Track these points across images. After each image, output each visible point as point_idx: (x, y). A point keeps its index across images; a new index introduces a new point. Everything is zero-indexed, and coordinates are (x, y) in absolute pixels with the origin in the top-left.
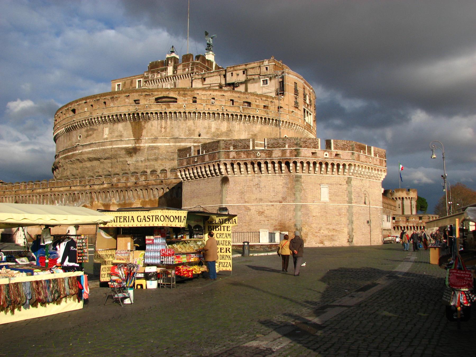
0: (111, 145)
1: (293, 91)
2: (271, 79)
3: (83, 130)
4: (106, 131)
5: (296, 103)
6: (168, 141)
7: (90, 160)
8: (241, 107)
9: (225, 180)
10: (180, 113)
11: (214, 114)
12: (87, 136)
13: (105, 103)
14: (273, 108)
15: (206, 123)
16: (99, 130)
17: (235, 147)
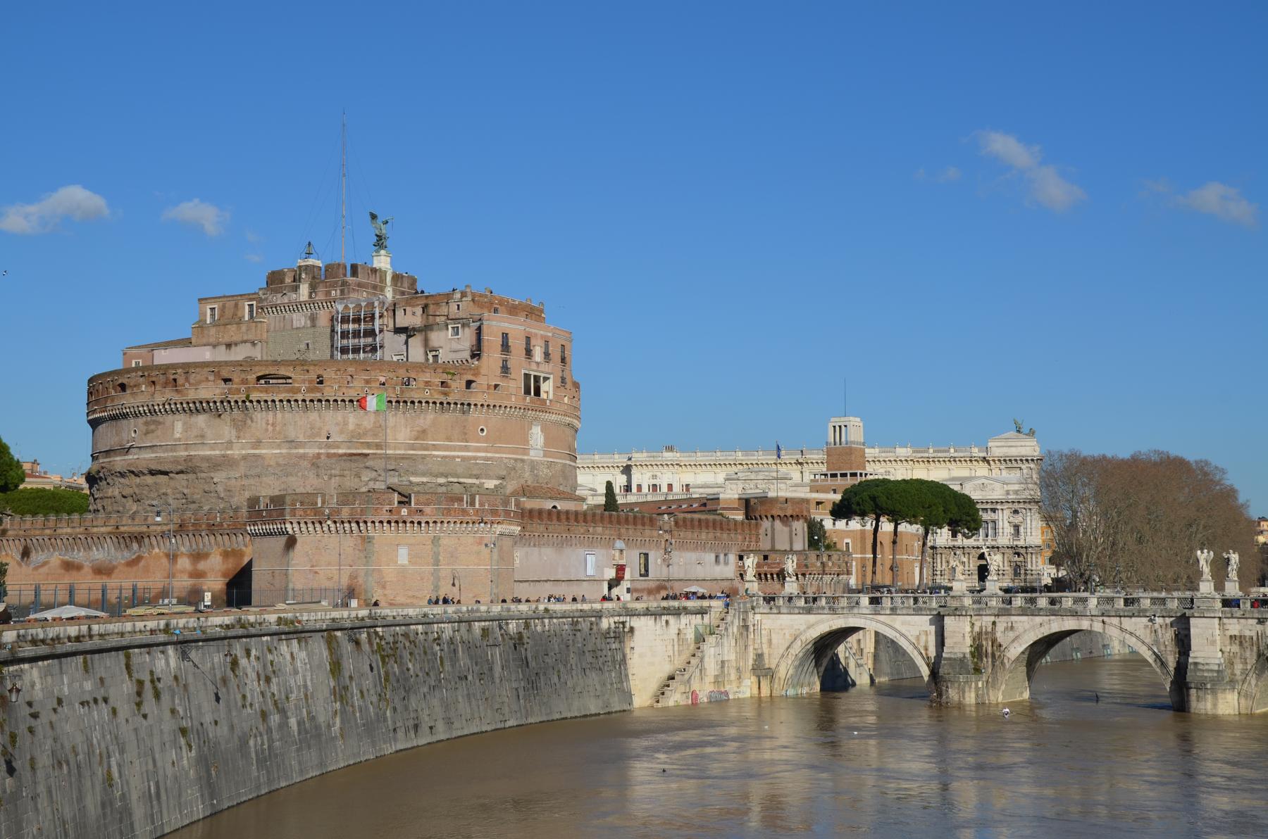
0: (186, 450)
1: (500, 348)
2: (463, 326)
3: (141, 420)
4: (179, 426)
5: (505, 369)
6: (279, 447)
7: (153, 473)
8: (398, 388)
9: (291, 542)
10: (296, 401)
11: (351, 401)
12: (147, 433)
13: (175, 380)
14: (457, 385)
15: (339, 415)
16: (168, 423)
17: (302, 503)
